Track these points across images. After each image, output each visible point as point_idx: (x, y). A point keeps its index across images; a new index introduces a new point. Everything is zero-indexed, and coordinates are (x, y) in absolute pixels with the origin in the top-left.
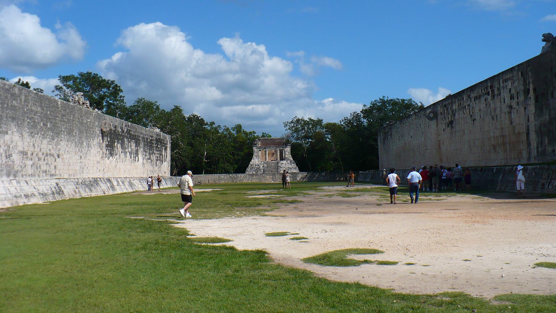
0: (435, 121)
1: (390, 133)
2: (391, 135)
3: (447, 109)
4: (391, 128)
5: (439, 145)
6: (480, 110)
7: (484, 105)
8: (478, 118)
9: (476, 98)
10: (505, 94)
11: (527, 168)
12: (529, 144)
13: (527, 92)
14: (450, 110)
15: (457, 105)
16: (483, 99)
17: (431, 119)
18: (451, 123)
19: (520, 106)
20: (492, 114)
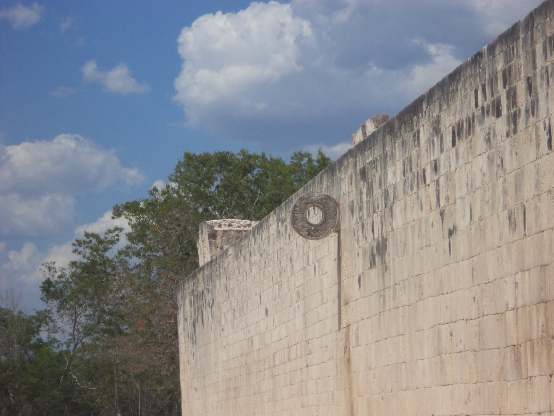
1: (208, 297)
3: (370, 189)
4: (210, 277)
5: (347, 349)
7: (482, 162)
8: (463, 223)
9: (458, 132)
14: (378, 192)
17: (314, 232)
18: (381, 248)
20: (511, 202)
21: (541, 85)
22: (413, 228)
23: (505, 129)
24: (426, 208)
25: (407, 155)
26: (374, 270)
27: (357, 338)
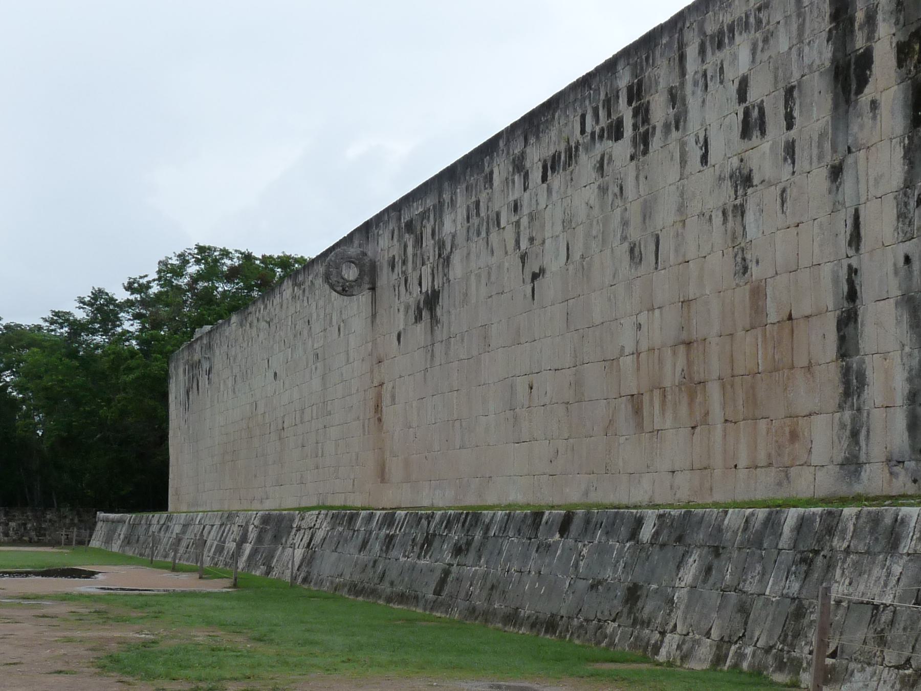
0: (363, 299)
1: (206, 365)
2: (209, 372)
3: (419, 241)
4: (210, 347)
5: (378, 408)
6: (568, 224)
7: (591, 194)
8: (554, 263)
9: (551, 166)
10: (713, 115)
11: (899, 523)
12: (852, 384)
13: (849, 75)
14: (428, 243)
15: (461, 212)
16: (586, 163)
17: (345, 290)
18: (432, 300)
19: (802, 161)
20: (634, 234)
21: (693, 93)
22: (479, 276)
23: (630, 150)
24: (498, 252)
25: (474, 199)
26: (419, 325)
27: (393, 397)
